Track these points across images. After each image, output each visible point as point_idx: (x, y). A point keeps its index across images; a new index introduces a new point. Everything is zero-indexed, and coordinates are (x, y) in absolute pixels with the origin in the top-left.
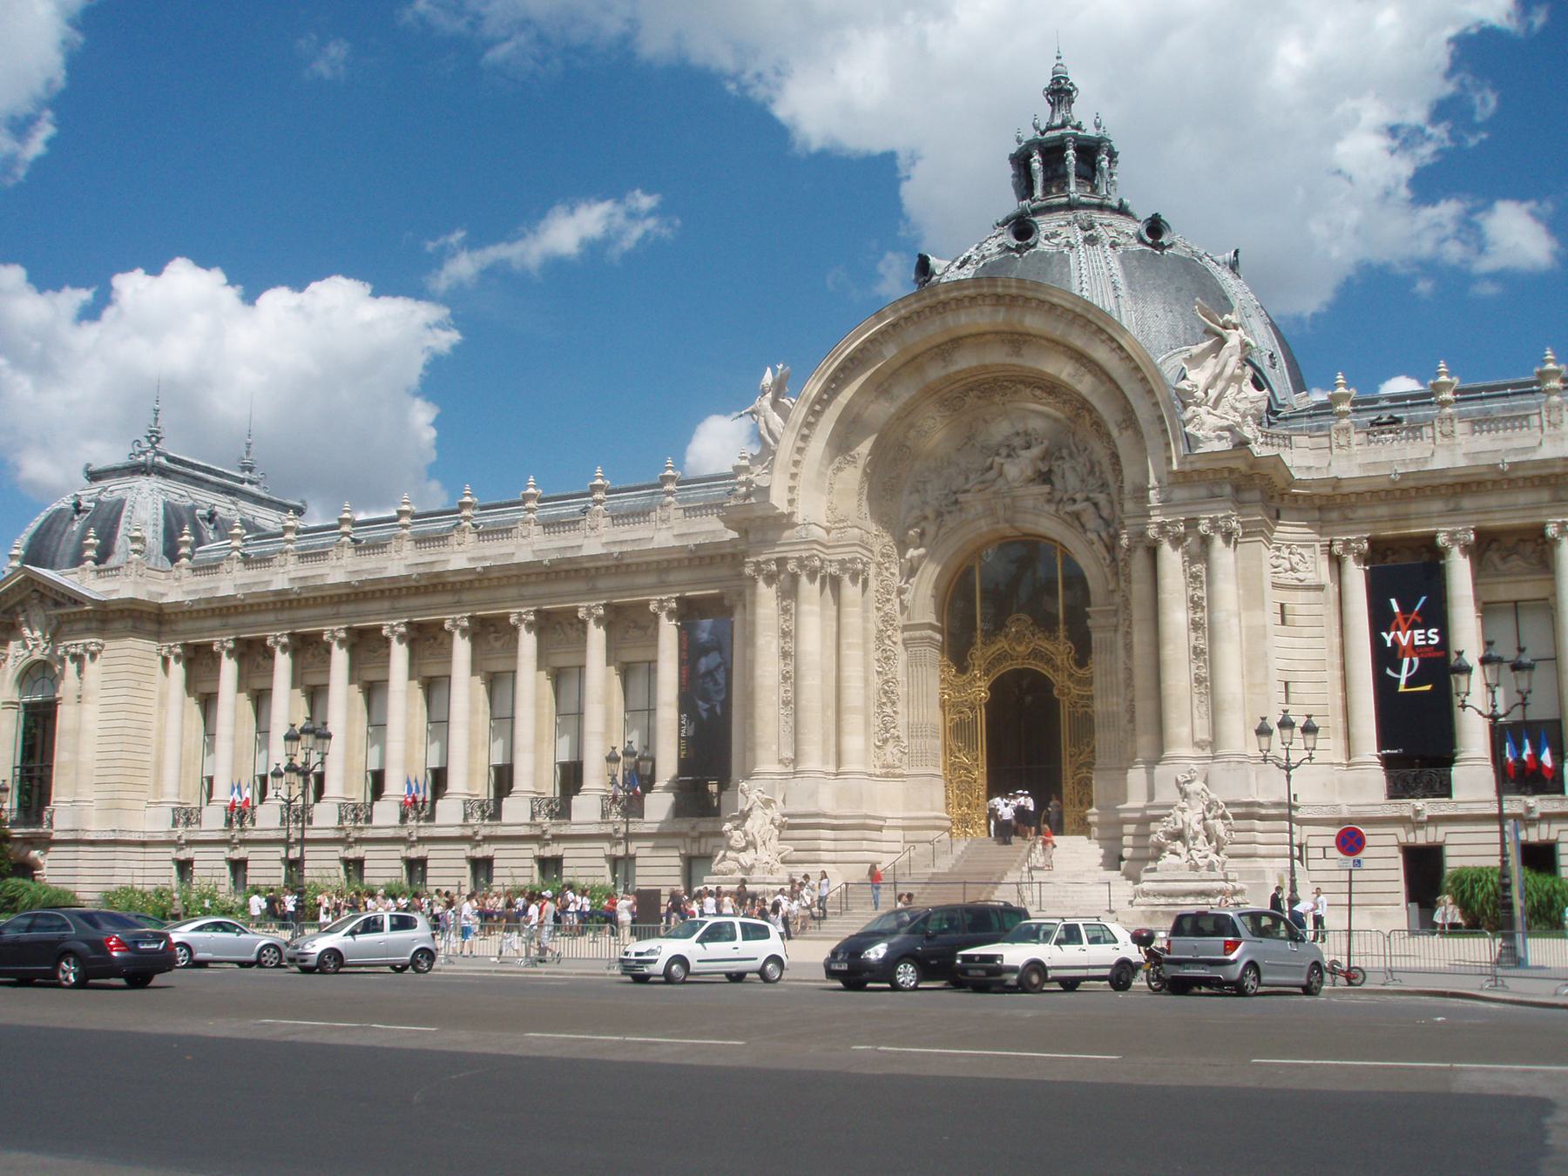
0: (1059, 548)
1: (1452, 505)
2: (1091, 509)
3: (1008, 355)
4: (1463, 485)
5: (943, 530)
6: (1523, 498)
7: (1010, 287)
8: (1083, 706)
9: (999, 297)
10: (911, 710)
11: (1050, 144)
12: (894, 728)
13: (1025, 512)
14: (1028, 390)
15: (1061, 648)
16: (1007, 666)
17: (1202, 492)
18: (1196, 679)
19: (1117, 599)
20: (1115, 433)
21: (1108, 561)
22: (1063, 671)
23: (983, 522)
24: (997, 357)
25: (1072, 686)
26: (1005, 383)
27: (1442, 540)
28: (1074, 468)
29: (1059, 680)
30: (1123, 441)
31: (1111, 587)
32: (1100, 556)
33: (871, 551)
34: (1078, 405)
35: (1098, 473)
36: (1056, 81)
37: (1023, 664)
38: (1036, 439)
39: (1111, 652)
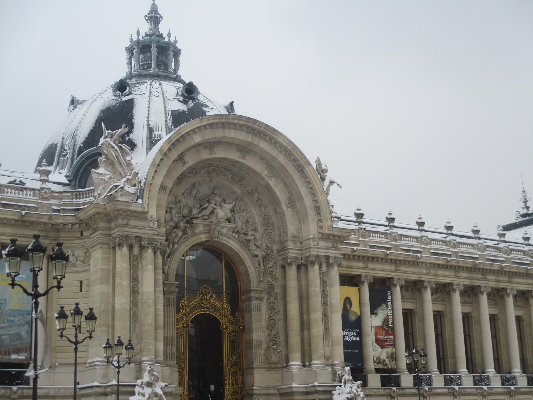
0: (224, 255)
1: (365, 266)
3: (239, 157)
4: (373, 258)
5: (187, 236)
6: (387, 267)
7: (261, 127)
8: (234, 336)
9: (253, 130)
10: (166, 330)
11: (162, 44)
13: (223, 235)
15: (225, 305)
16: (199, 312)
17: (330, 245)
18: (325, 328)
19: (264, 285)
20: (284, 208)
21: (262, 267)
22: (225, 317)
23: (203, 236)
24: (234, 155)
25: (229, 325)
26: (222, 169)
27: (363, 278)
28: (239, 217)
29: (224, 321)
30: (288, 214)
31: (261, 279)
32: (257, 263)
34: (254, 189)
35: (251, 223)
36: (152, 11)
37: (207, 311)
38: (229, 199)
39: (260, 311)
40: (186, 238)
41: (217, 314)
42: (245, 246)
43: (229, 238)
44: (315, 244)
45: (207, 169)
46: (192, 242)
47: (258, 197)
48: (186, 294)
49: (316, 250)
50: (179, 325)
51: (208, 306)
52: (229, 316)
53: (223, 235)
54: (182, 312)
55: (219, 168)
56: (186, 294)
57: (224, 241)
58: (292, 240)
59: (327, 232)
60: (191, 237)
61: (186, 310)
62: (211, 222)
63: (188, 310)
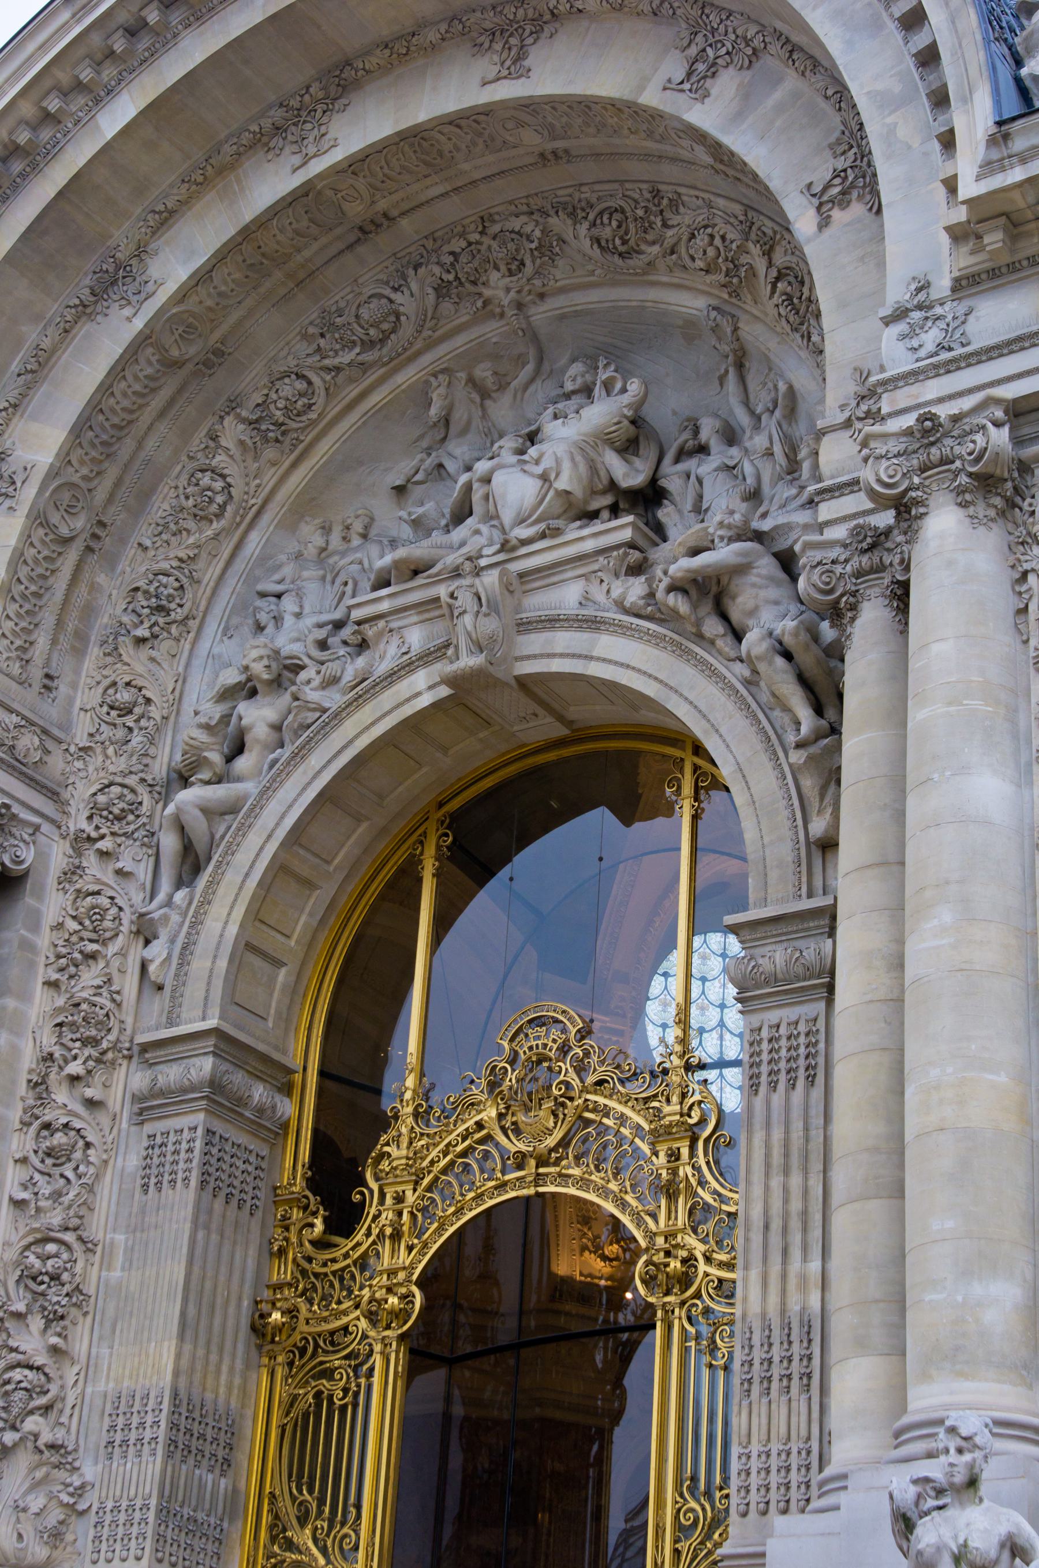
2: (766, 565)
12: (47, 1409)
13: (552, 622)
14: (583, 229)
22: (672, 1196)
23: (420, 679)
25: (699, 1249)
33: (53, 795)
39: (811, 1080)
40: (309, 726)
41: (613, 1186)
42: (699, 637)
43: (593, 624)
44: (922, 353)
45: (422, 271)
46: (351, 742)
47: (770, 264)
48: (408, 1095)
49: (932, 389)
50: (345, 1313)
51: (551, 1141)
52: (702, 1183)
53: (552, 622)
54: (376, 1217)
55: (496, 228)
56: (408, 1095)
57: (562, 655)
58: (848, 424)
59: (969, 188)
60: (338, 716)
61: (399, 1199)
62: (456, 573)
63: (410, 1198)
